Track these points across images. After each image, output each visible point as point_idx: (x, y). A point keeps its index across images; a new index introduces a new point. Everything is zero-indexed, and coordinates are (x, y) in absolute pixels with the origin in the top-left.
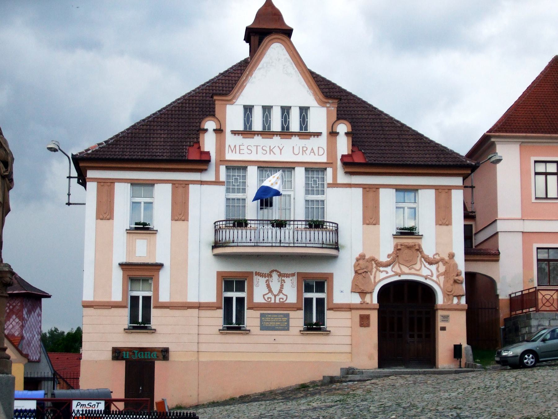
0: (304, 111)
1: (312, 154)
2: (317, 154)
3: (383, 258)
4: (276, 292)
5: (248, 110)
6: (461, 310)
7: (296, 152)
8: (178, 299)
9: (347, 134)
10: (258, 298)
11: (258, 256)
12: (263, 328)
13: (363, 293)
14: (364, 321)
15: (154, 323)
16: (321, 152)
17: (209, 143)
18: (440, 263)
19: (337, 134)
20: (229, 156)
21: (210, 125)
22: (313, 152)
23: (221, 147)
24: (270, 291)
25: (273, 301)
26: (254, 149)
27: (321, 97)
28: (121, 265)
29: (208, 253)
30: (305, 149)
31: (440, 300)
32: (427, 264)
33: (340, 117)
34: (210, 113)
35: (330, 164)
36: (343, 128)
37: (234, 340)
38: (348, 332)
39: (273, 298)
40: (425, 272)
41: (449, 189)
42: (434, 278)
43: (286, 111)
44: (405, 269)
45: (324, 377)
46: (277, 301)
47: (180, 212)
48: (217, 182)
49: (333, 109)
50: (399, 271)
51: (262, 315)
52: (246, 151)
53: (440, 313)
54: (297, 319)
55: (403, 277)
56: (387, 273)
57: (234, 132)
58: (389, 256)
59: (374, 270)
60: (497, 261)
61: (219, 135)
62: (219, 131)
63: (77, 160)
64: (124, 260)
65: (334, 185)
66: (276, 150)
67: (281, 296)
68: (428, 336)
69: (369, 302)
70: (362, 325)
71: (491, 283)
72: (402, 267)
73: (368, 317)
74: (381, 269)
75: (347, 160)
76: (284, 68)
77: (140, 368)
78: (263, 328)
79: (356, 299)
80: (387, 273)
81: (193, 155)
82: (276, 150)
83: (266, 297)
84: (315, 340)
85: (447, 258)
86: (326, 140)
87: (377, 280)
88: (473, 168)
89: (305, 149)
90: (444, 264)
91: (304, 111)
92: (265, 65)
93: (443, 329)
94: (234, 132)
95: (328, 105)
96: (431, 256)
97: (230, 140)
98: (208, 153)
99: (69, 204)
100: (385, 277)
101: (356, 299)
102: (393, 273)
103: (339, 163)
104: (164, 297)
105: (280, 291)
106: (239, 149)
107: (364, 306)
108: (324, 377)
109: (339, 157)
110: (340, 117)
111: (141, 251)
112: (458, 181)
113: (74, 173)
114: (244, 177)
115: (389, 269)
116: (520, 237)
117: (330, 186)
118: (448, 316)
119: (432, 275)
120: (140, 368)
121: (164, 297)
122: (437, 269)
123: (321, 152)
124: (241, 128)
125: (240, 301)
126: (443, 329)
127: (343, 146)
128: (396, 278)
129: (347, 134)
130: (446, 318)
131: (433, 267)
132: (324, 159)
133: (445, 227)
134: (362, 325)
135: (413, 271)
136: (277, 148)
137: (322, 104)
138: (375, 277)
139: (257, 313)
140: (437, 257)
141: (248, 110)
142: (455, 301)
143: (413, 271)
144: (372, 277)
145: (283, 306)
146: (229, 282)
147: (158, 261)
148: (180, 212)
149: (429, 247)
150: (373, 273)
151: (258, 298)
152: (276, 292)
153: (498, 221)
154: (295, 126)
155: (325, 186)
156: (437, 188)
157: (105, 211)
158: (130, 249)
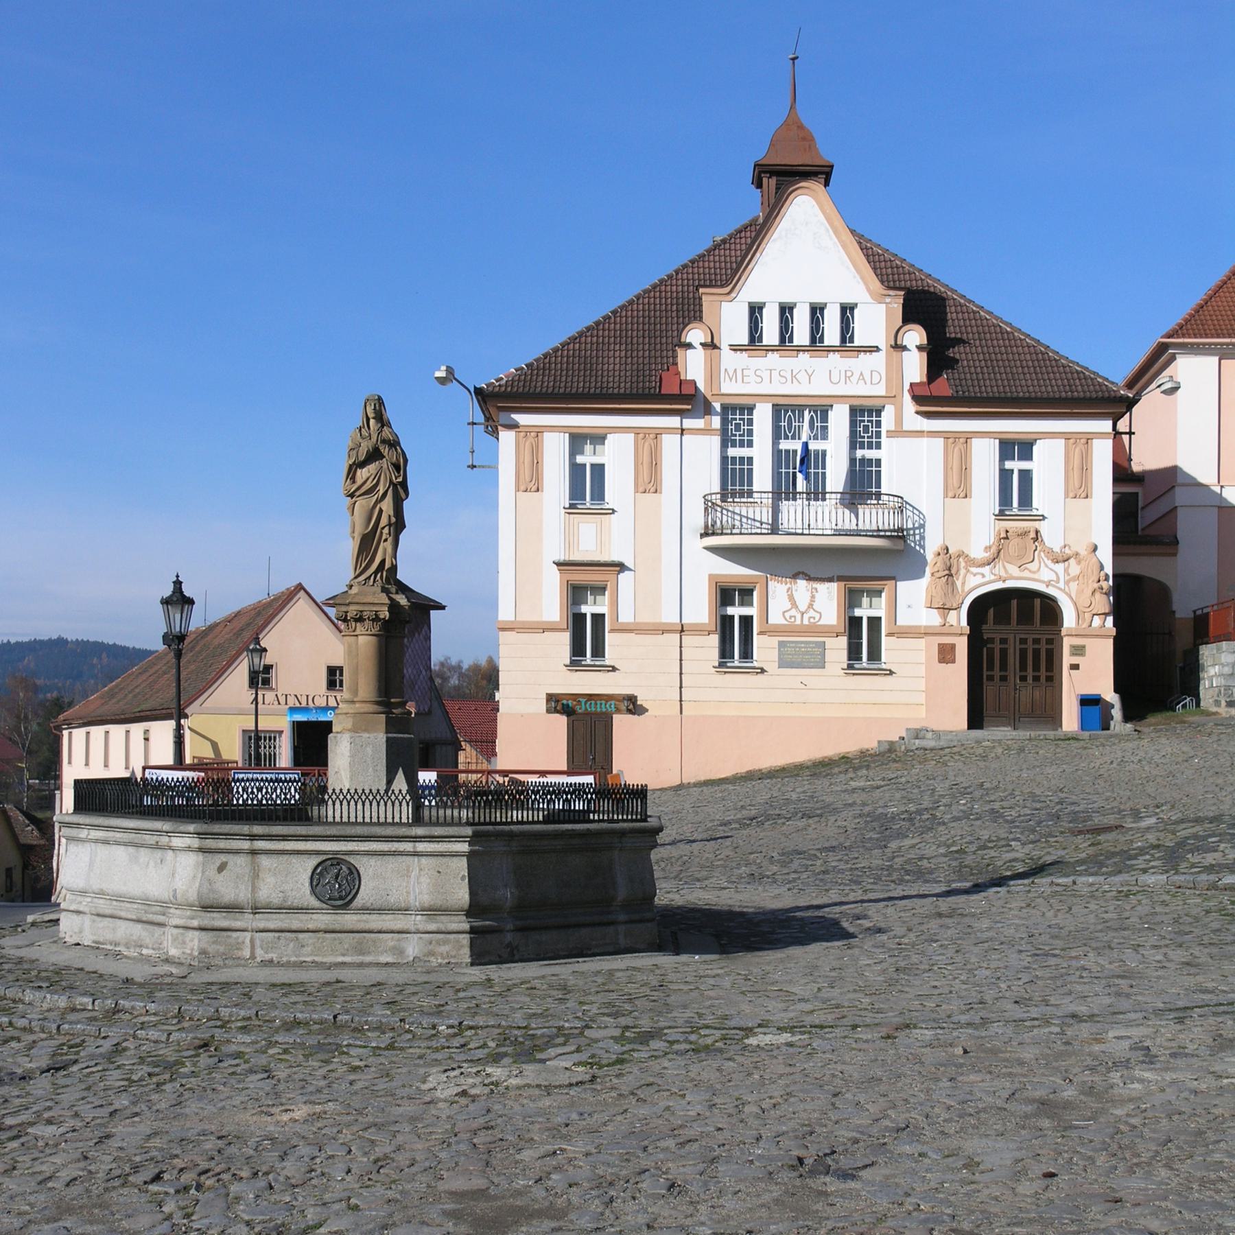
0: (847, 311)
1: (861, 382)
3: (978, 553)
4: (803, 607)
5: (755, 311)
6: (1107, 637)
7: (835, 379)
8: (646, 618)
9: (920, 348)
10: (775, 618)
12: (783, 664)
13: (945, 609)
14: (946, 654)
15: (610, 657)
16: (876, 378)
17: (693, 366)
18: (1072, 561)
19: (904, 348)
20: (728, 387)
21: (695, 335)
23: (713, 372)
24: (794, 605)
25: (798, 622)
26: (766, 375)
27: (876, 284)
28: (558, 564)
29: (695, 545)
30: (849, 374)
31: (1069, 619)
32: (1049, 562)
33: (910, 316)
35: (891, 398)
36: (915, 336)
37: (737, 684)
38: (922, 671)
39: (799, 616)
40: (1046, 575)
41: (1089, 438)
42: (1061, 585)
43: (817, 311)
44: (1013, 570)
45: (879, 742)
46: (806, 622)
47: (649, 477)
48: (707, 431)
50: (1003, 574)
51: (781, 644)
52: (753, 378)
53: (1067, 643)
54: (838, 648)
55: (1010, 584)
56: (983, 576)
57: (735, 348)
58: (987, 549)
59: (963, 572)
60: (1175, 555)
61: (709, 352)
62: (711, 345)
63: (483, 396)
64: (562, 557)
65: (898, 433)
66: (803, 377)
67: (812, 613)
68: (1049, 679)
69: (955, 623)
70: (942, 660)
71: (1163, 592)
72: (1008, 566)
73: (953, 647)
74: (974, 570)
75: (919, 392)
77: (589, 725)
78: (783, 664)
79: (932, 619)
80: (983, 576)
81: (670, 388)
82: (803, 377)
83: (787, 615)
84: (865, 686)
85: (1083, 553)
86: (885, 359)
87: (966, 589)
88: (1130, 404)
89: (849, 374)
90: (1079, 563)
91: (847, 311)
93: (1075, 667)
94: (735, 348)
95: (888, 300)
96: (1057, 549)
97: (729, 359)
98: (694, 382)
99: (473, 467)
100: (978, 582)
101: (932, 619)
102: (993, 577)
103: (907, 397)
104: (626, 616)
105: (811, 606)
107: (945, 630)
108: (879, 742)
109: (907, 387)
110: (910, 316)
111: (591, 540)
112: (1106, 425)
113: (480, 418)
114: (750, 422)
115: (986, 570)
116: (1216, 510)
117: (890, 434)
118: (1084, 647)
119: (1058, 581)
120: (589, 725)
121: (626, 616)
122: (1066, 570)
123: (876, 378)
124: (744, 339)
125: (747, 621)
126: (1075, 667)
127: (914, 367)
128: (999, 585)
129: (920, 348)
130: (1078, 650)
131: (1060, 568)
132: (881, 390)
133: (1081, 502)
134: (942, 660)
135: (1026, 574)
136: (803, 372)
137: (879, 299)
138: (963, 584)
139: (774, 641)
140: (1067, 551)
141: (755, 311)
142: (1097, 621)
143: (1026, 574)
144: (959, 583)
145: (815, 630)
146: (726, 594)
147: (615, 558)
148: (649, 477)
149: (1052, 535)
150: (961, 577)
151: (775, 618)
152: (803, 607)
153: (1177, 489)
154: (832, 334)
155: (884, 434)
156: (1067, 436)
157: (531, 480)
158: (569, 538)
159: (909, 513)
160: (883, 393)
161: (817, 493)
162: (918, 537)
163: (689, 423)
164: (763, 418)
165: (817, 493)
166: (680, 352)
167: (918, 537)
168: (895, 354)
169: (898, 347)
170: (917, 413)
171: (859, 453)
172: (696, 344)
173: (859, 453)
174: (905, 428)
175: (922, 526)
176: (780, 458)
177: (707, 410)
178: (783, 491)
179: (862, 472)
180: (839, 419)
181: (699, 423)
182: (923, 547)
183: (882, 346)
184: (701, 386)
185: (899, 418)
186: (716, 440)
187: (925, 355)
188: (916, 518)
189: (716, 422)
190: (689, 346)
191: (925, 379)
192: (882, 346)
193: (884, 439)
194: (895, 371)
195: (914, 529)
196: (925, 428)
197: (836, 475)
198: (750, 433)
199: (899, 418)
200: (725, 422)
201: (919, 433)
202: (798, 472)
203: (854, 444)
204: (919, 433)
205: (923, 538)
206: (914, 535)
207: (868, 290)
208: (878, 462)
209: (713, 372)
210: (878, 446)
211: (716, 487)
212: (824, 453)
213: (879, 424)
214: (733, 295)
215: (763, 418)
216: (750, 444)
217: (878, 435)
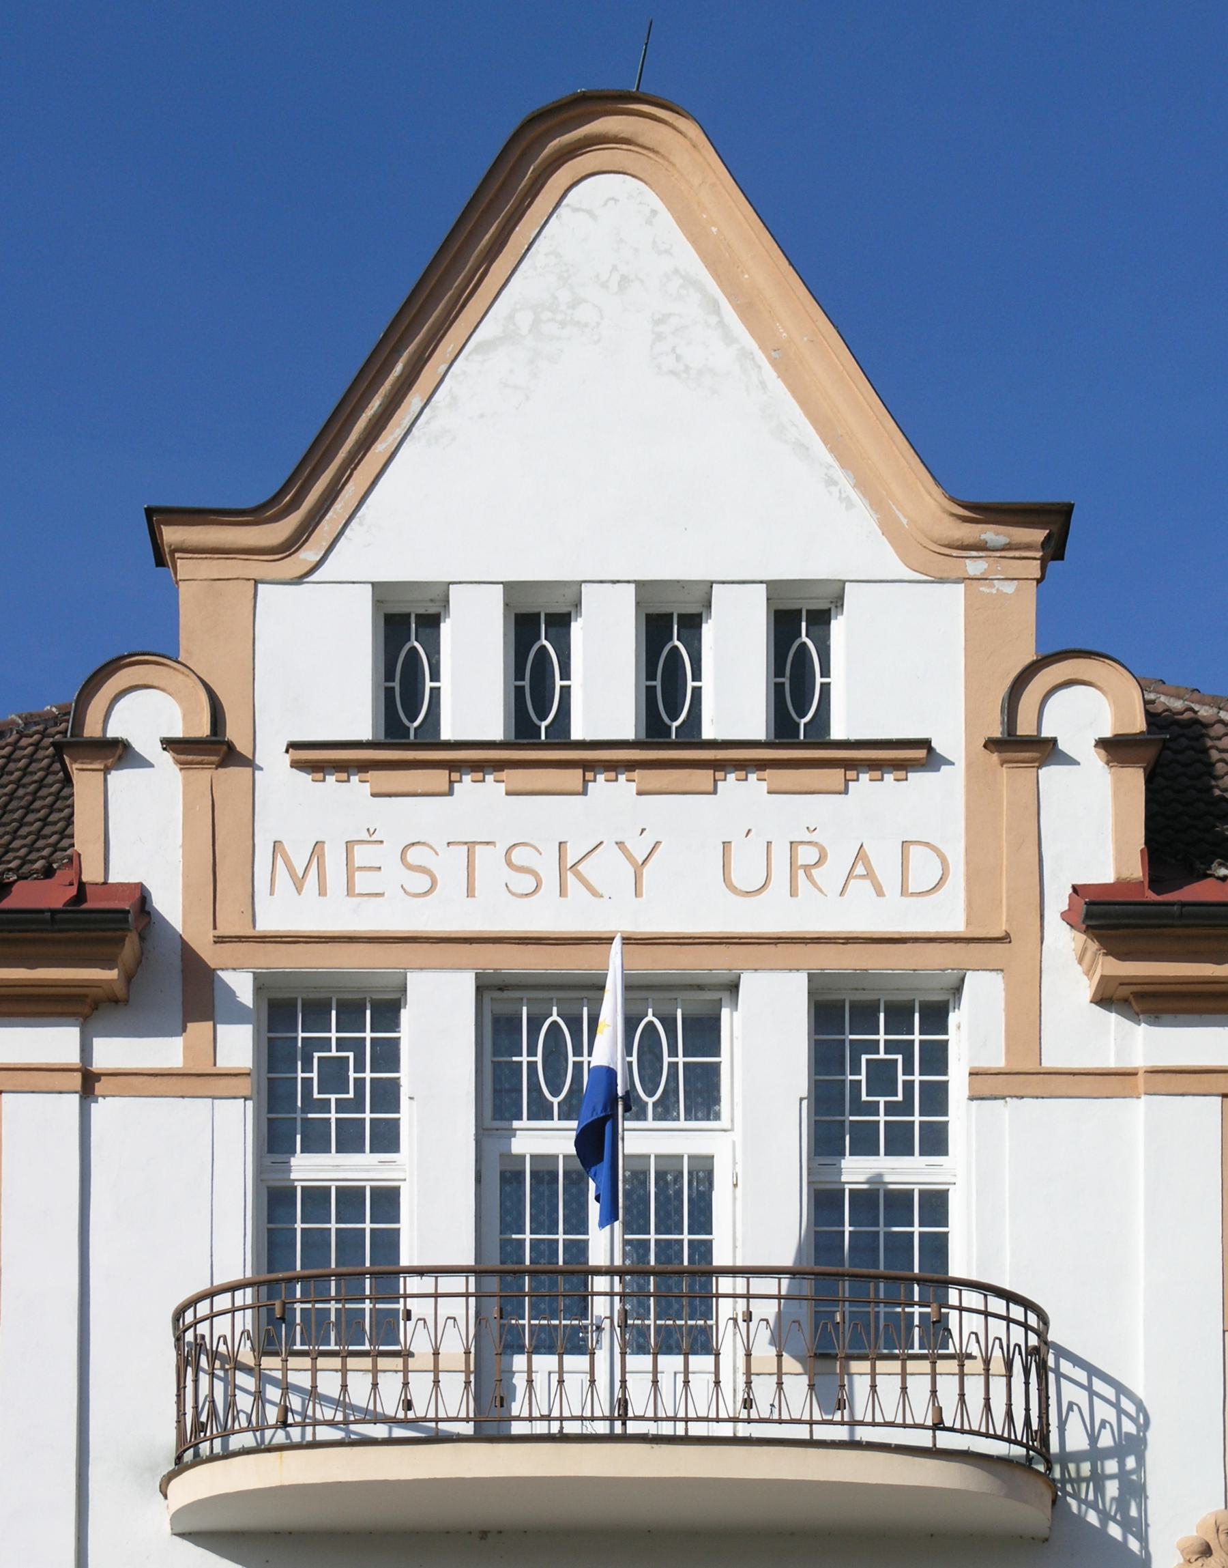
2: (891, 883)
11: (484, 1534)
16: (924, 870)
17: (138, 832)
19: (1045, 750)
21: (146, 714)
22: (870, 875)
23: (220, 852)
30: (807, 855)
34: (151, 645)
49: (1009, 588)
57: (318, 759)
61: (203, 776)
66: (609, 870)
76: (659, 337)
82: (609, 870)
89: (807, 855)
92: (524, 320)
94: (318, 759)
95: (975, 567)
97: (288, 805)
103: (1063, 946)
106: (352, 867)
109: (1058, 900)
114: (388, 1055)
117: (989, 1085)
123: (924, 870)
132: (947, 914)
136: (610, 853)
137: (938, 561)
159: (1071, 1393)
160: (957, 925)
161: (676, 1297)
162: (1112, 1488)
163: (112, 1052)
164: (438, 1035)
165: (676, 1297)
166: (85, 781)
167: (1112, 1488)
168: (1008, 779)
169: (1020, 747)
170: (1104, 999)
171: (856, 1170)
172: (146, 744)
173: (856, 1170)
174: (1049, 1062)
175: (1134, 1445)
176: (505, 1188)
177: (199, 997)
178: (527, 1294)
179: (865, 1245)
180: (766, 1042)
181: (166, 1052)
182: (1137, 1527)
183: (951, 739)
184: (170, 905)
185: (1025, 1019)
186: (234, 1122)
187: (1135, 778)
188: (1104, 1412)
189: (237, 1045)
190: (118, 753)
191: (1136, 870)
192: (951, 739)
193: (961, 1114)
194: (1006, 846)
195: (1095, 1454)
196: (1139, 1059)
197: (758, 1217)
198: (387, 1096)
199: (1025, 1019)
200: (276, 1055)
201: (1115, 1081)
202: (581, 1241)
203: (833, 1124)
204: (1115, 1081)
205: (1134, 1489)
206: (1098, 1479)
207: (889, 528)
208: (936, 1204)
209: (220, 852)
210: (936, 1142)
211: (235, 1257)
212: (703, 1171)
213: (936, 1058)
214: (309, 555)
215: (438, 1035)
216: (387, 1139)
217: (936, 1098)
